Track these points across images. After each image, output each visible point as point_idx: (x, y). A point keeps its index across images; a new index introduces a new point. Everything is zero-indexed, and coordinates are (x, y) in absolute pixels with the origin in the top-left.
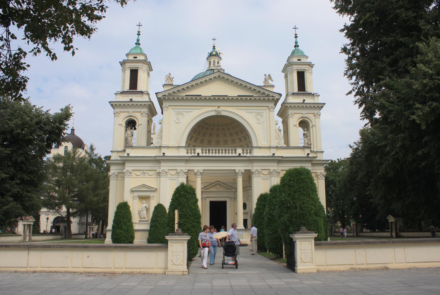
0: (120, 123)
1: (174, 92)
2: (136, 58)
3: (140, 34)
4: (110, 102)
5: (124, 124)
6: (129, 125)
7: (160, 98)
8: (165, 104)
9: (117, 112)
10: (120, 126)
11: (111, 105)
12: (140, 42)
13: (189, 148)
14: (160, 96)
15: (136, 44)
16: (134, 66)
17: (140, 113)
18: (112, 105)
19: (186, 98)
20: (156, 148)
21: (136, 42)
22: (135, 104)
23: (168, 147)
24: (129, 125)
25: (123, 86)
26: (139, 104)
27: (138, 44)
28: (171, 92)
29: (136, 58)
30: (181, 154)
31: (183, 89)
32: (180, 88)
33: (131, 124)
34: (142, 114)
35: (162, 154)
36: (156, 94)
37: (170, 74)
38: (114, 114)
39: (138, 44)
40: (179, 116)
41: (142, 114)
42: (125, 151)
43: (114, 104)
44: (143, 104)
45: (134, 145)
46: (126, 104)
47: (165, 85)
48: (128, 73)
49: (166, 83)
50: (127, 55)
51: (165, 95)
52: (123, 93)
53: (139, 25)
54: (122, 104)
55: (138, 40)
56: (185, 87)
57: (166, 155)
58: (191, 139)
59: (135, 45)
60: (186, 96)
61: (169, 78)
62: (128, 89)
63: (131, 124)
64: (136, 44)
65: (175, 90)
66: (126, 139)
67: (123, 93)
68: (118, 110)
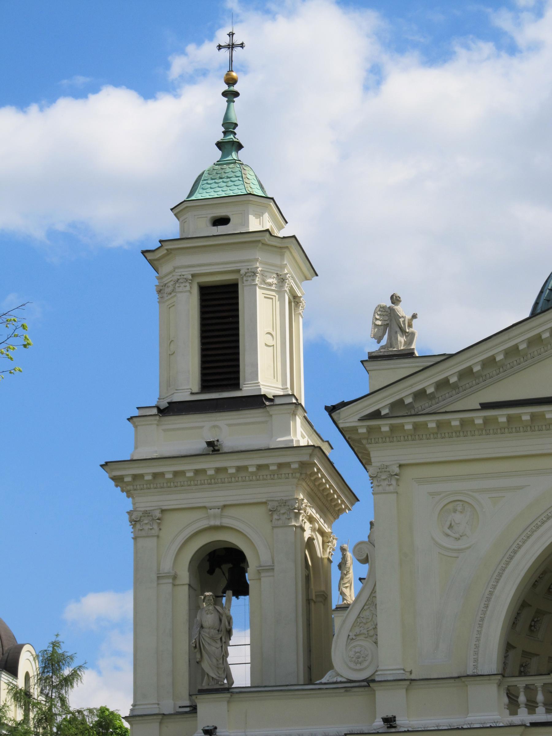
0: (167, 566)
1: (420, 394)
2: (223, 221)
3: (236, 94)
4: (105, 465)
5: (184, 576)
6: (211, 572)
7: (354, 429)
8: (381, 455)
9: (147, 513)
10: (167, 587)
11: (114, 478)
12: (240, 135)
13: (521, 682)
14: (350, 418)
15: (220, 145)
16: (215, 266)
17: (261, 511)
18: (118, 480)
19: (486, 420)
20: (350, 686)
21: (220, 137)
22: (231, 463)
23: (410, 682)
24: (211, 572)
25: (168, 382)
26: (252, 462)
27: (229, 145)
28: (405, 392)
29: (223, 221)
30: (476, 718)
31: (467, 373)
32: (450, 372)
33: (226, 567)
34: (273, 511)
35: (379, 723)
36: (331, 410)
37: (395, 299)
38: (134, 522)
39: (229, 145)
40: (457, 517)
41: (273, 511)
42: (194, 709)
43: (128, 472)
44: (272, 460)
45: (241, 676)
46: (189, 467)
47: (373, 357)
48: (189, 306)
49: (374, 347)
50: (179, 210)
51: (376, 415)
52: (171, 409)
53: (231, 47)
54: (168, 469)
55: (229, 126)
56: (474, 363)
57: (402, 721)
58: (532, 628)
59: (218, 154)
60: (485, 406)
61: (389, 320)
62: (196, 387)
63: (223, 569)
64: (220, 145)
65: (427, 382)
66: (197, 648)
67: (171, 409)
68: (151, 501)
